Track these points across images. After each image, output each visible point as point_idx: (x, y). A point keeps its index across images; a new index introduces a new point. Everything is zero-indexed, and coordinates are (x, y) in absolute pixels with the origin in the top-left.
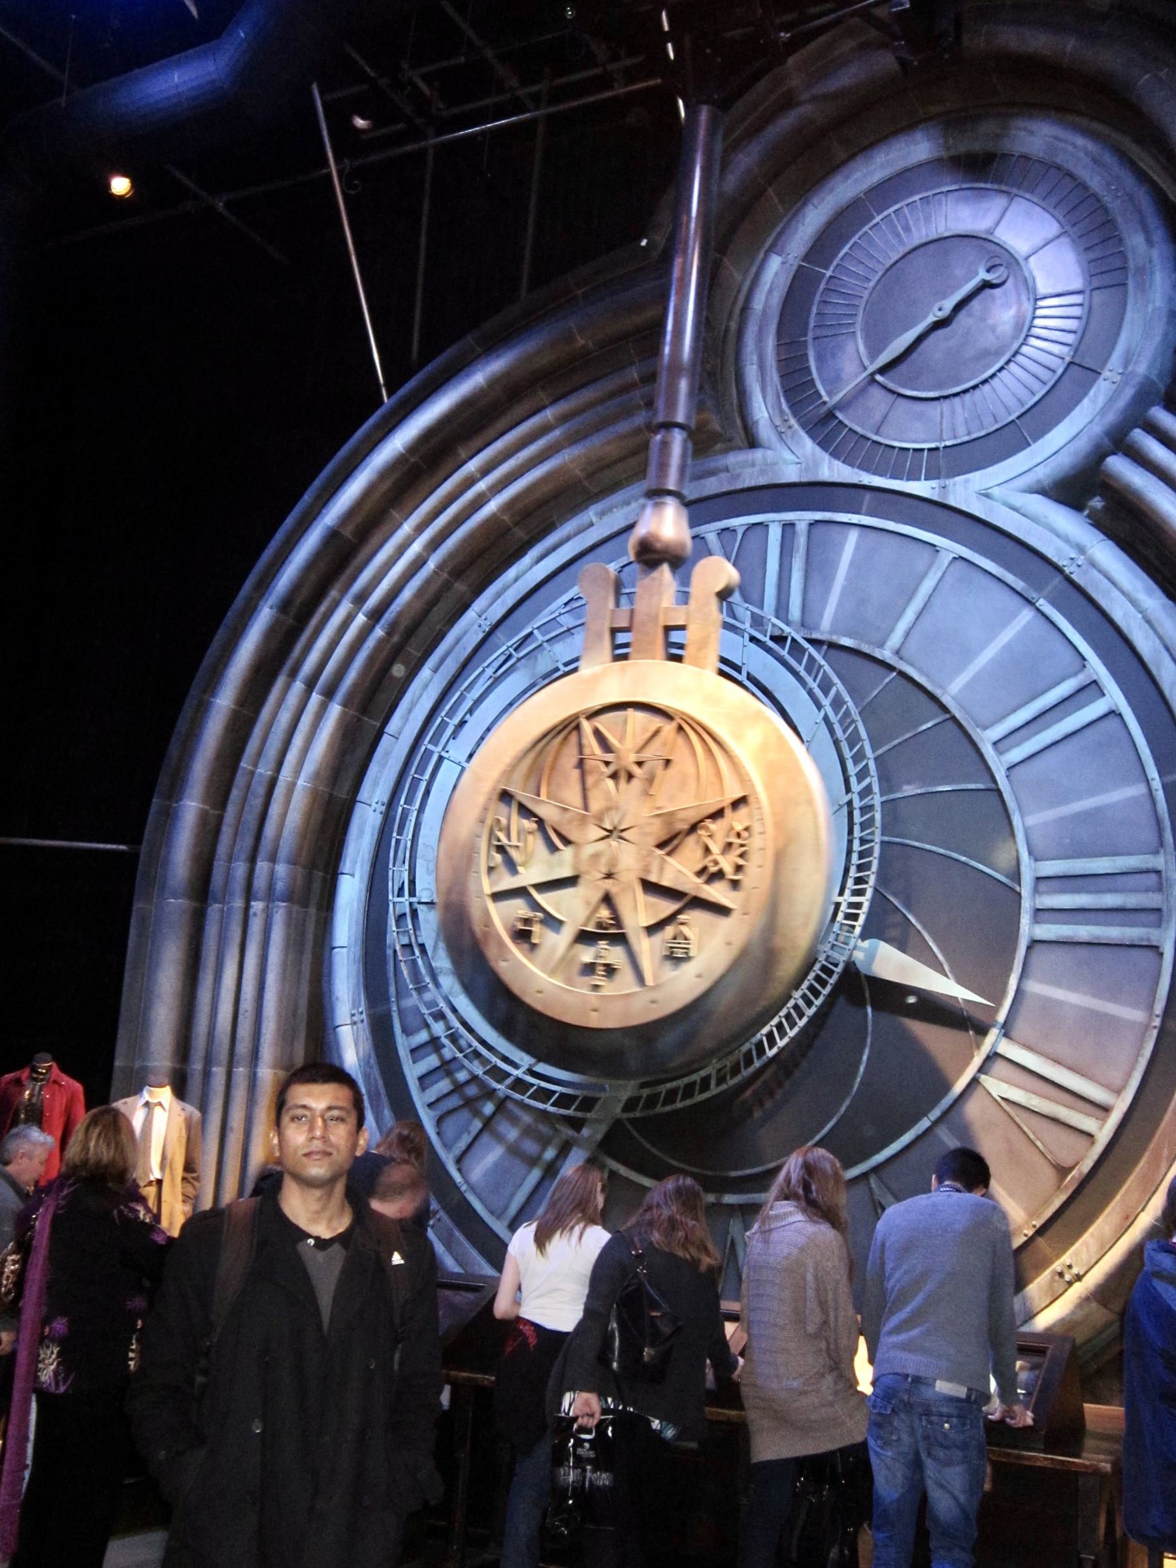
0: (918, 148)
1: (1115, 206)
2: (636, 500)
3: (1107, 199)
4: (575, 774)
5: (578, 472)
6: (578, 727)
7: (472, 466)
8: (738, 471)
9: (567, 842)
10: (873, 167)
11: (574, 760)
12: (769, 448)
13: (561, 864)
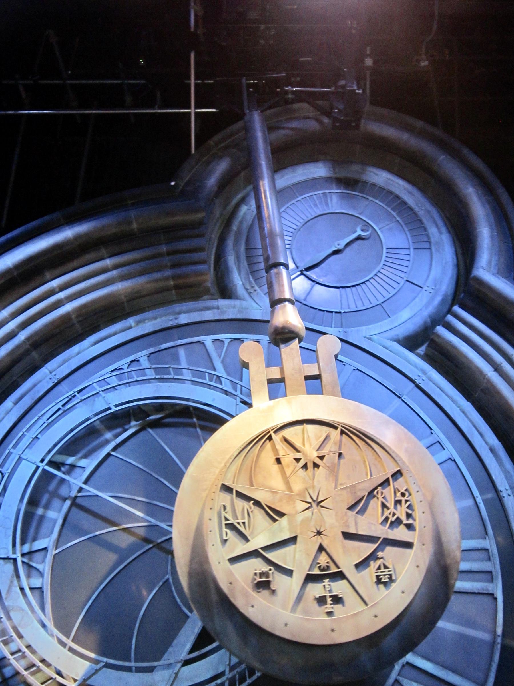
0: (319, 170)
1: (421, 213)
2: (161, 317)
3: (417, 210)
4: (276, 467)
5: (123, 297)
6: (270, 438)
7: (55, 283)
8: (225, 309)
9: (281, 515)
10: (296, 174)
11: (273, 460)
12: (243, 300)
13: (281, 530)
